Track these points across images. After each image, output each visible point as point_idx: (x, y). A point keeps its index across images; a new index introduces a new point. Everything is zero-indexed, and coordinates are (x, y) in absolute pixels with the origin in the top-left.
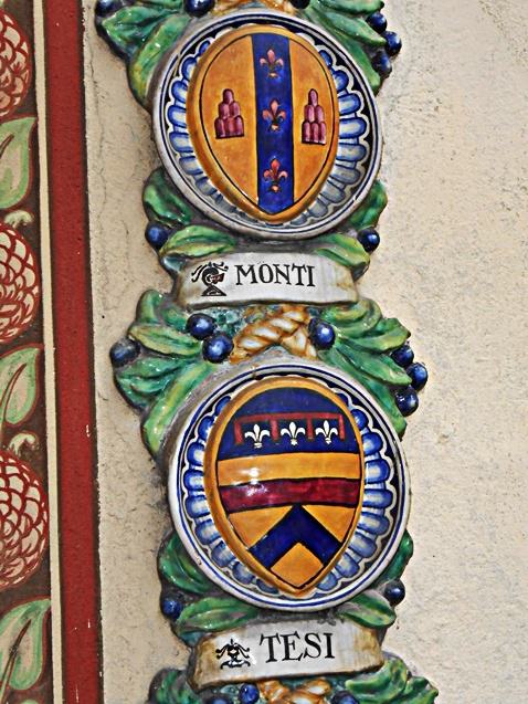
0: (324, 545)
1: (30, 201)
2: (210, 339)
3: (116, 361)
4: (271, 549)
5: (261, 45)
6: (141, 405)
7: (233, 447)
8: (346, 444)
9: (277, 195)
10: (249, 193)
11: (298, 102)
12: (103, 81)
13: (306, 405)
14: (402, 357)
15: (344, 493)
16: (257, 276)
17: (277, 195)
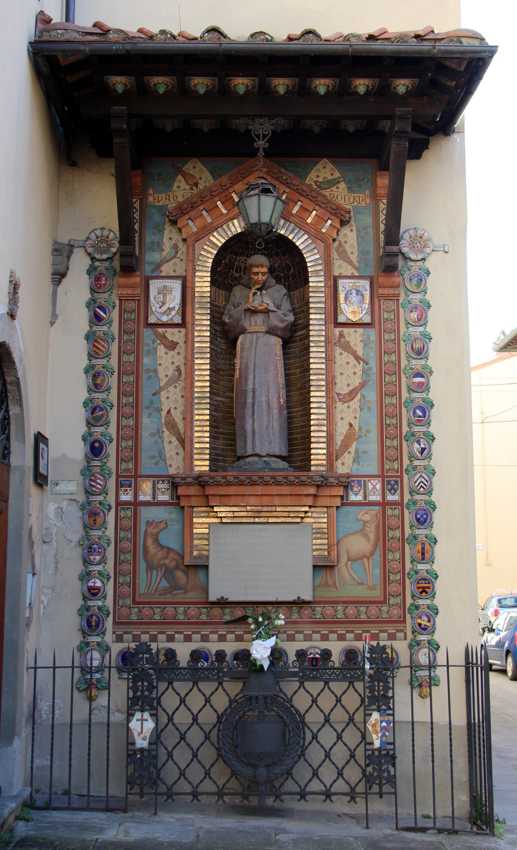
0: (426, 592)
1: (400, 559)
2: (416, 572)
3: (408, 574)
4: (421, 593)
5: (422, 543)
6: (410, 579)
7: (418, 583)
8: (429, 583)
9: (423, 559)
10: (421, 558)
11: (426, 549)
12: (407, 546)
13: (425, 579)
14: (436, 574)
15: (429, 588)
16: (421, 567)
17: (423, 559)
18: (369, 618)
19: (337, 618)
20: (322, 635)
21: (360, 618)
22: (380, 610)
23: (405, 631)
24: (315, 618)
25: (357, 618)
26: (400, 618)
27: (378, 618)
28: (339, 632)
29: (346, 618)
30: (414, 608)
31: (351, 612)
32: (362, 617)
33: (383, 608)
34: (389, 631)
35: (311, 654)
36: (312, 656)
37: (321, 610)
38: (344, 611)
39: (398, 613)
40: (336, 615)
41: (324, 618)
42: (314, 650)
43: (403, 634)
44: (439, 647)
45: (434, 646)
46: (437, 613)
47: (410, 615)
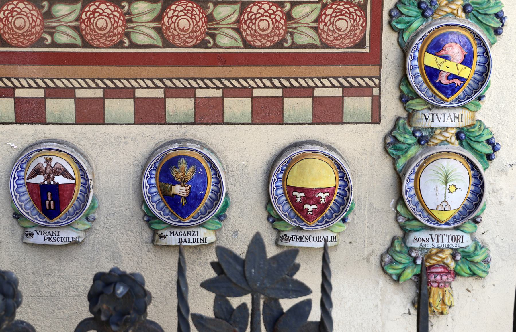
18: (247, 44)
19: (133, 45)
20: (80, 103)
21: (216, 46)
22: (289, 16)
23: (376, 91)
24: (54, 44)
25: (203, 44)
26: (361, 44)
27: (280, 44)
28: (139, 93)
29: (167, 44)
30: (414, 12)
31: (184, 23)
32: (222, 40)
33: (299, 11)
34: (317, 93)
35: (36, 172)
36: (39, 179)
37: (73, 16)
38: (159, 18)
39: (354, 28)
40: (127, 35)
41: (86, 44)
42: (48, 161)
43: (367, 101)
44: (495, 149)
45: (478, 147)
46: (497, 32)
47: (395, 36)
